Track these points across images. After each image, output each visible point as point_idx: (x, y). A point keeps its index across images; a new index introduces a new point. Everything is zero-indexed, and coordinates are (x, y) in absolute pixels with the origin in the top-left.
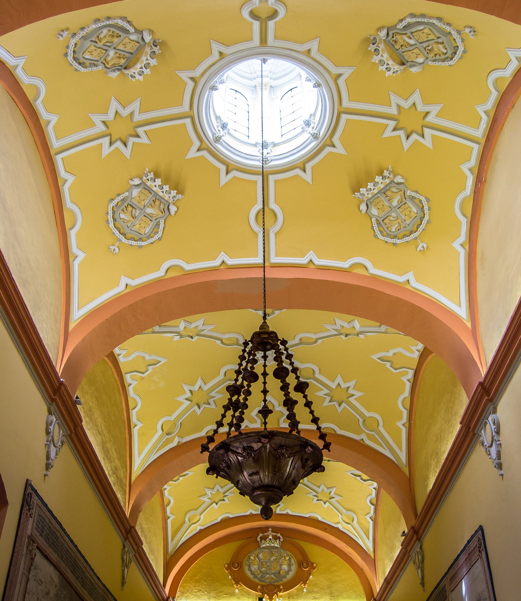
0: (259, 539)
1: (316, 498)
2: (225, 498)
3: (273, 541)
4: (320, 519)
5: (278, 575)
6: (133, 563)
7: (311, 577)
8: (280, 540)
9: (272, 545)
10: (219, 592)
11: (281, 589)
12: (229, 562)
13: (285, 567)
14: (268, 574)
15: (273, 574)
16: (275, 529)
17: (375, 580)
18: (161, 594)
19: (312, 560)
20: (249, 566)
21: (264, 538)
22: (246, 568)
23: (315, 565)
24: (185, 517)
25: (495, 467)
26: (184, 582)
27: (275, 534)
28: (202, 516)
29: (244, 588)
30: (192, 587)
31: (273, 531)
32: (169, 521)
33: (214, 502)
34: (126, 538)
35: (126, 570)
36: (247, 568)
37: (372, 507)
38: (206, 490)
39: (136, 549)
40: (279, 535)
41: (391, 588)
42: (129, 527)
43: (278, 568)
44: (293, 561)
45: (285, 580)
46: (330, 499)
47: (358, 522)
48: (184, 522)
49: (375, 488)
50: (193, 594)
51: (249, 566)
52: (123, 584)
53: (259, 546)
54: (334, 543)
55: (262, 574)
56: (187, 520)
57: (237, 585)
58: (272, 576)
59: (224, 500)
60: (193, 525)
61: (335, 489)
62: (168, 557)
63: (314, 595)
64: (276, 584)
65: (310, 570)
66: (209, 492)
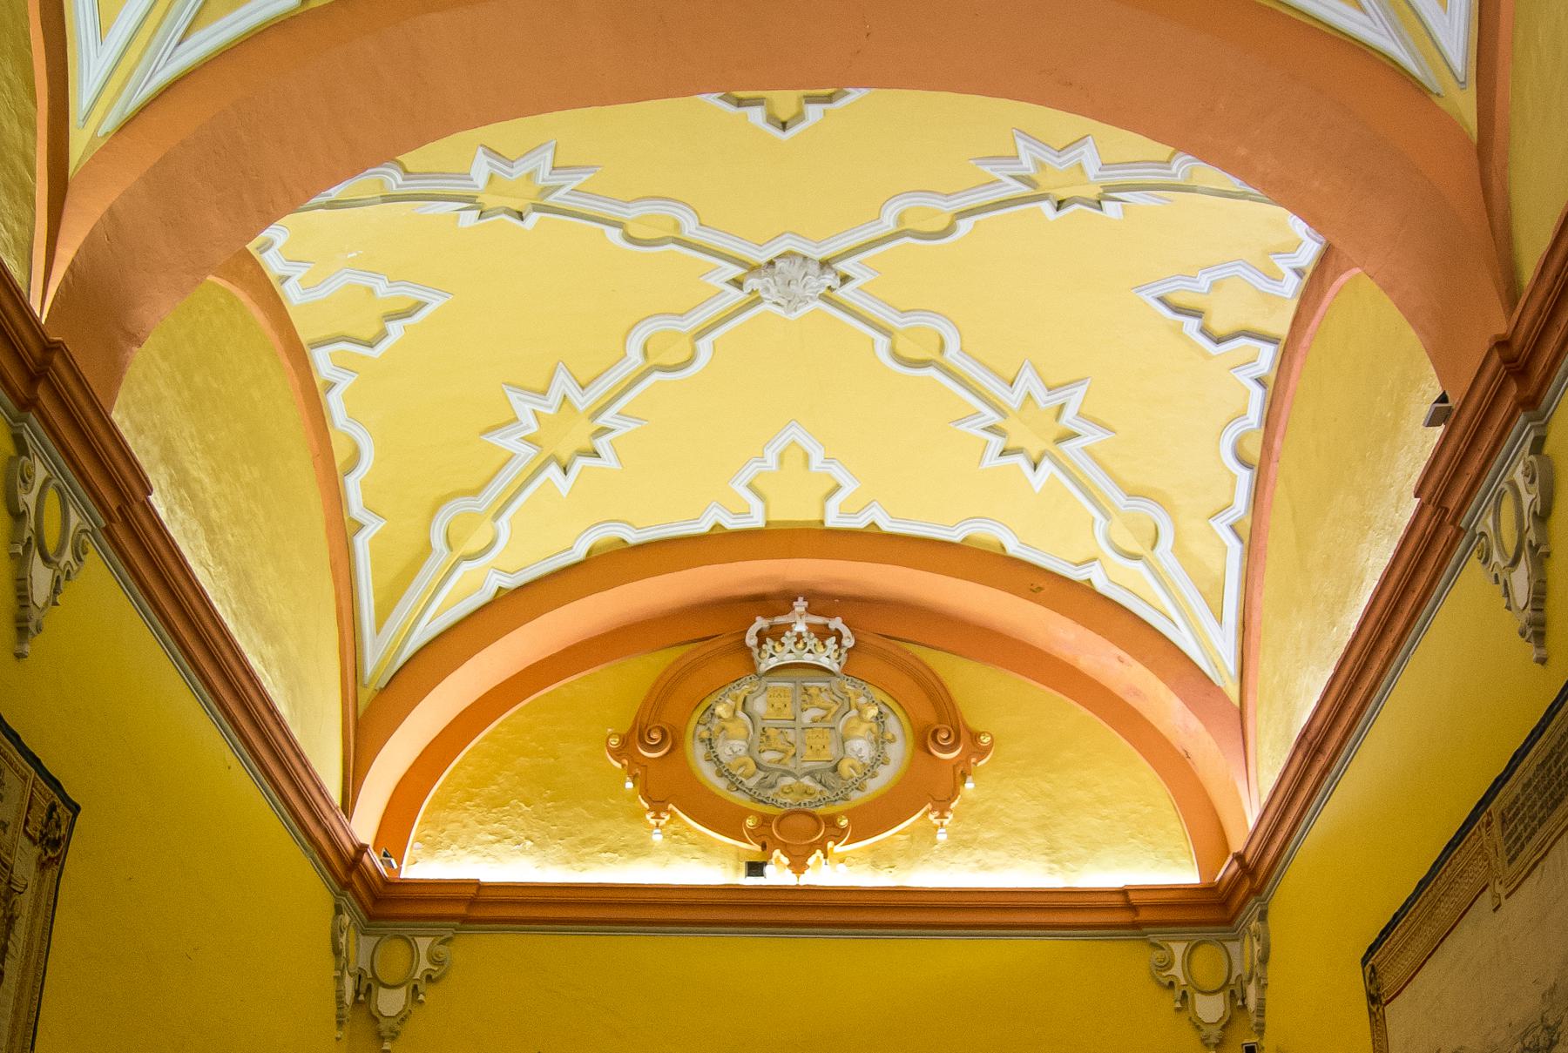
0: (751, 641)
1: (997, 443)
2: (602, 444)
3: (812, 642)
4: (1013, 549)
5: (830, 778)
6: (93, 558)
7: (969, 785)
8: (839, 642)
9: (808, 659)
10: (584, 843)
11: (844, 831)
12: (625, 730)
13: (861, 747)
14: (788, 773)
15: (811, 774)
16: (822, 601)
17: (1241, 786)
18: (319, 822)
19: (975, 723)
20: (709, 742)
21: (776, 633)
22: (696, 753)
23: (986, 740)
24: (428, 529)
25: (1522, 634)
26: (440, 804)
27: (819, 620)
28: (504, 521)
29: (689, 829)
30: (471, 822)
31: (809, 611)
32: (362, 543)
33: (553, 458)
34: (27, 404)
35: (41, 577)
36: (700, 750)
37: (1244, 477)
38: (513, 396)
39: (112, 503)
40: (836, 623)
41: (1326, 770)
42: (36, 349)
43: (832, 752)
44: (893, 726)
45: (857, 797)
46: (1061, 439)
47: (1178, 549)
48: (428, 548)
49: (1260, 381)
50: (475, 852)
51: (709, 742)
52: (23, 628)
53: (753, 668)
54: (1065, 654)
55: (762, 774)
56: (438, 542)
57: (657, 817)
58: (807, 781)
59: (596, 454)
60: (466, 566)
61: (1080, 391)
62: (365, 697)
63: (979, 854)
64: (822, 810)
65: (964, 760)
66: (524, 408)
